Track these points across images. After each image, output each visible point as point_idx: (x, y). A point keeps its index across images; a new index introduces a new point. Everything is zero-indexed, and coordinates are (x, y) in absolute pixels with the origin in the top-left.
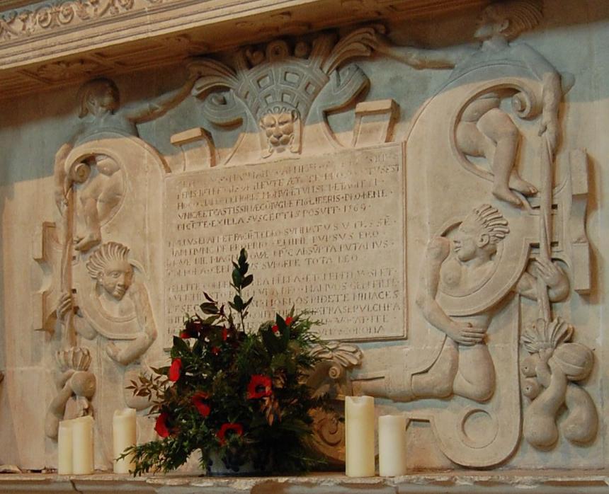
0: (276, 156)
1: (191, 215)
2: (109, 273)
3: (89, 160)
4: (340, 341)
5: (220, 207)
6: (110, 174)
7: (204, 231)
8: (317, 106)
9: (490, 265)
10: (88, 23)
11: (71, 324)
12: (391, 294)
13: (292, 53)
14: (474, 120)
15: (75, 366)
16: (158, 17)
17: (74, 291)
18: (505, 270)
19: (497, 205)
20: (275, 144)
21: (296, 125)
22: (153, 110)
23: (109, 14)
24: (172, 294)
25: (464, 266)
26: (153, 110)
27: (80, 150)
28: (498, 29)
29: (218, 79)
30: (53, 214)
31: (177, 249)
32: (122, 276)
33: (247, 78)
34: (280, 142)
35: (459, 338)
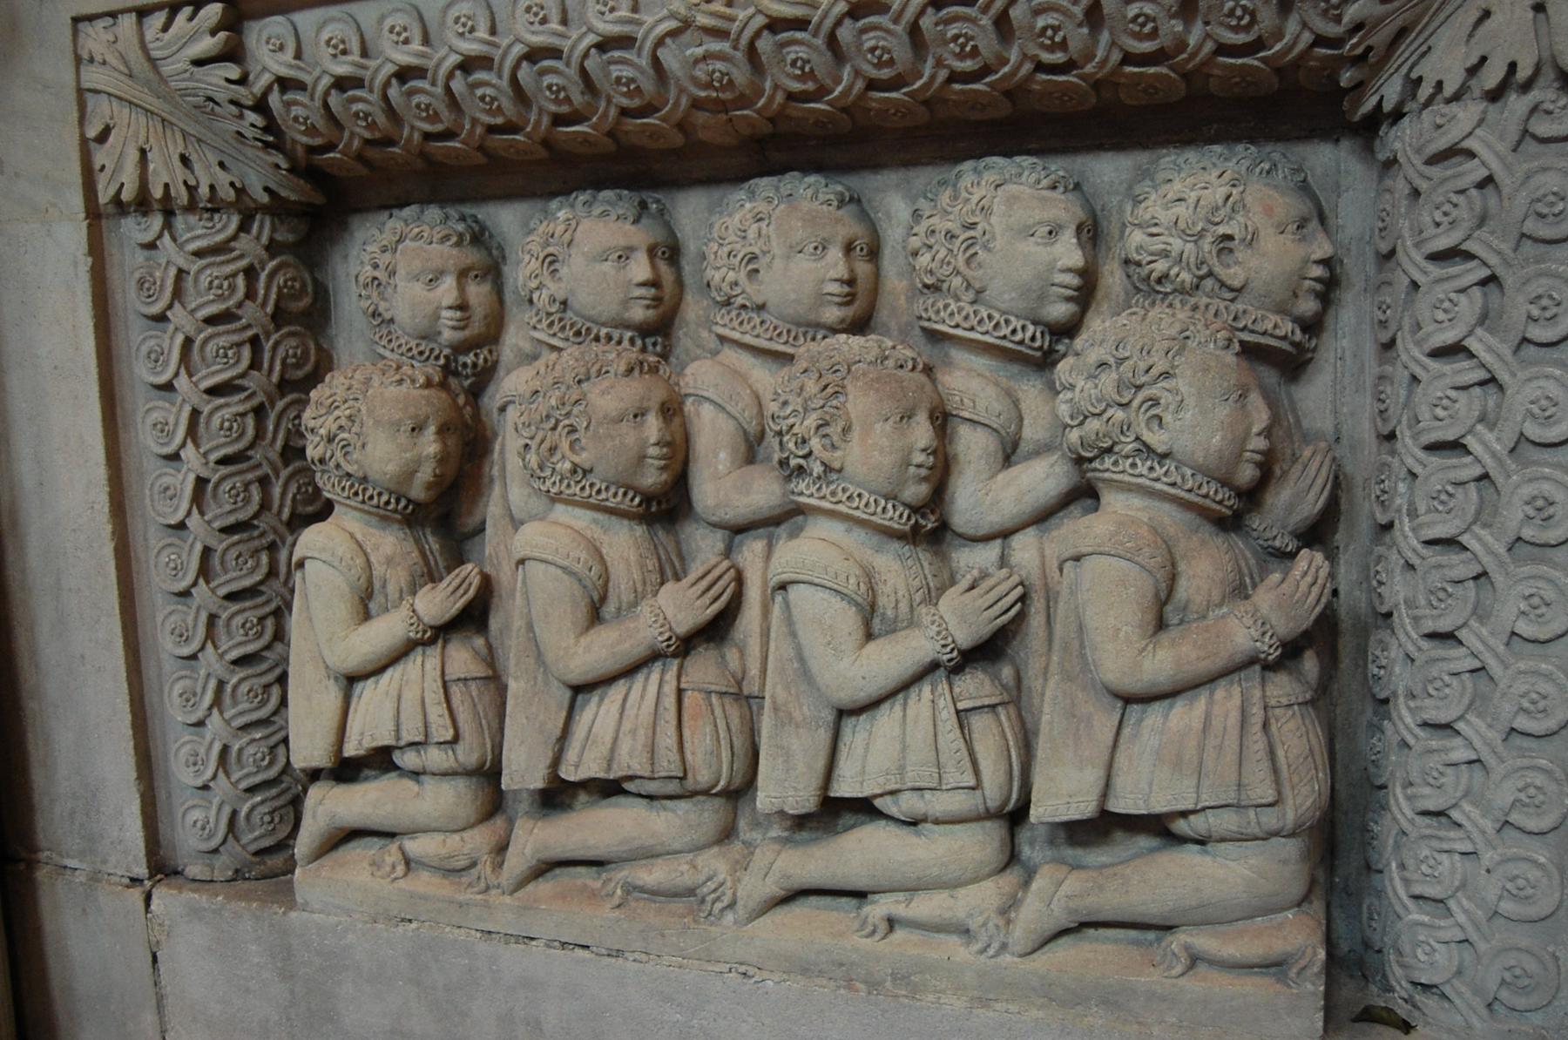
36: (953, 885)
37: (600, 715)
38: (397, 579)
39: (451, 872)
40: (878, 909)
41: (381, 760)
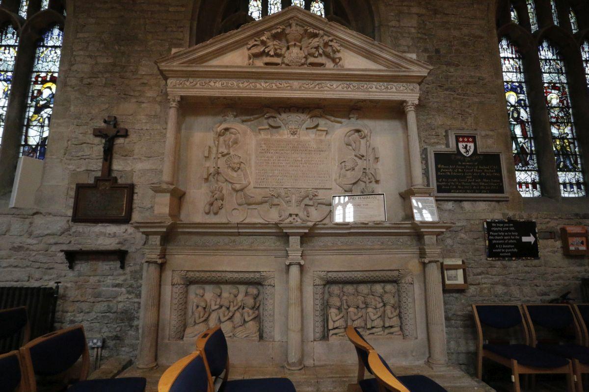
0: (292, 137)
1: (264, 150)
2: (234, 163)
3: (227, 129)
4: (312, 188)
5: (274, 148)
6: (235, 134)
7: (270, 155)
8: (304, 126)
9: (353, 172)
10: (239, 88)
11: (217, 177)
12: (328, 177)
13: (297, 111)
14: (350, 136)
15: (218, 191)
16: (266, 91)
17: (219, 168)
18: (358, 174)
19: (355, 158)
20: (292, 134)
21: (299, 130)
22: (250, 118)
23: (248, 87)
24: (257, 171)
25: (347, 172)
26: (250, 118)
27: (224, 126)
28: (356, 116)
29: (273, 114)
30: (210, 142)
31: (259, 159)
32: (238, 165)
33: (284, 116)
34: (294, 133)
35: (347, 189)
36: (379, 332)
37: (356, 322)
38: (338, 314)
39: (342, 336)
40: (376, 334)
41: (337, 328)
